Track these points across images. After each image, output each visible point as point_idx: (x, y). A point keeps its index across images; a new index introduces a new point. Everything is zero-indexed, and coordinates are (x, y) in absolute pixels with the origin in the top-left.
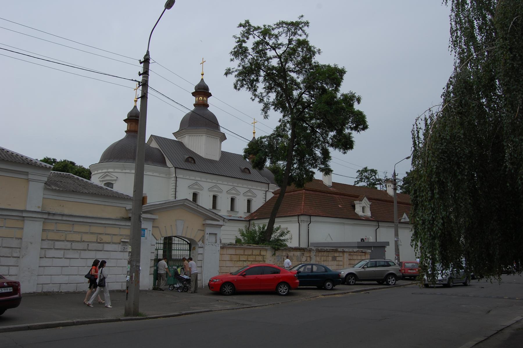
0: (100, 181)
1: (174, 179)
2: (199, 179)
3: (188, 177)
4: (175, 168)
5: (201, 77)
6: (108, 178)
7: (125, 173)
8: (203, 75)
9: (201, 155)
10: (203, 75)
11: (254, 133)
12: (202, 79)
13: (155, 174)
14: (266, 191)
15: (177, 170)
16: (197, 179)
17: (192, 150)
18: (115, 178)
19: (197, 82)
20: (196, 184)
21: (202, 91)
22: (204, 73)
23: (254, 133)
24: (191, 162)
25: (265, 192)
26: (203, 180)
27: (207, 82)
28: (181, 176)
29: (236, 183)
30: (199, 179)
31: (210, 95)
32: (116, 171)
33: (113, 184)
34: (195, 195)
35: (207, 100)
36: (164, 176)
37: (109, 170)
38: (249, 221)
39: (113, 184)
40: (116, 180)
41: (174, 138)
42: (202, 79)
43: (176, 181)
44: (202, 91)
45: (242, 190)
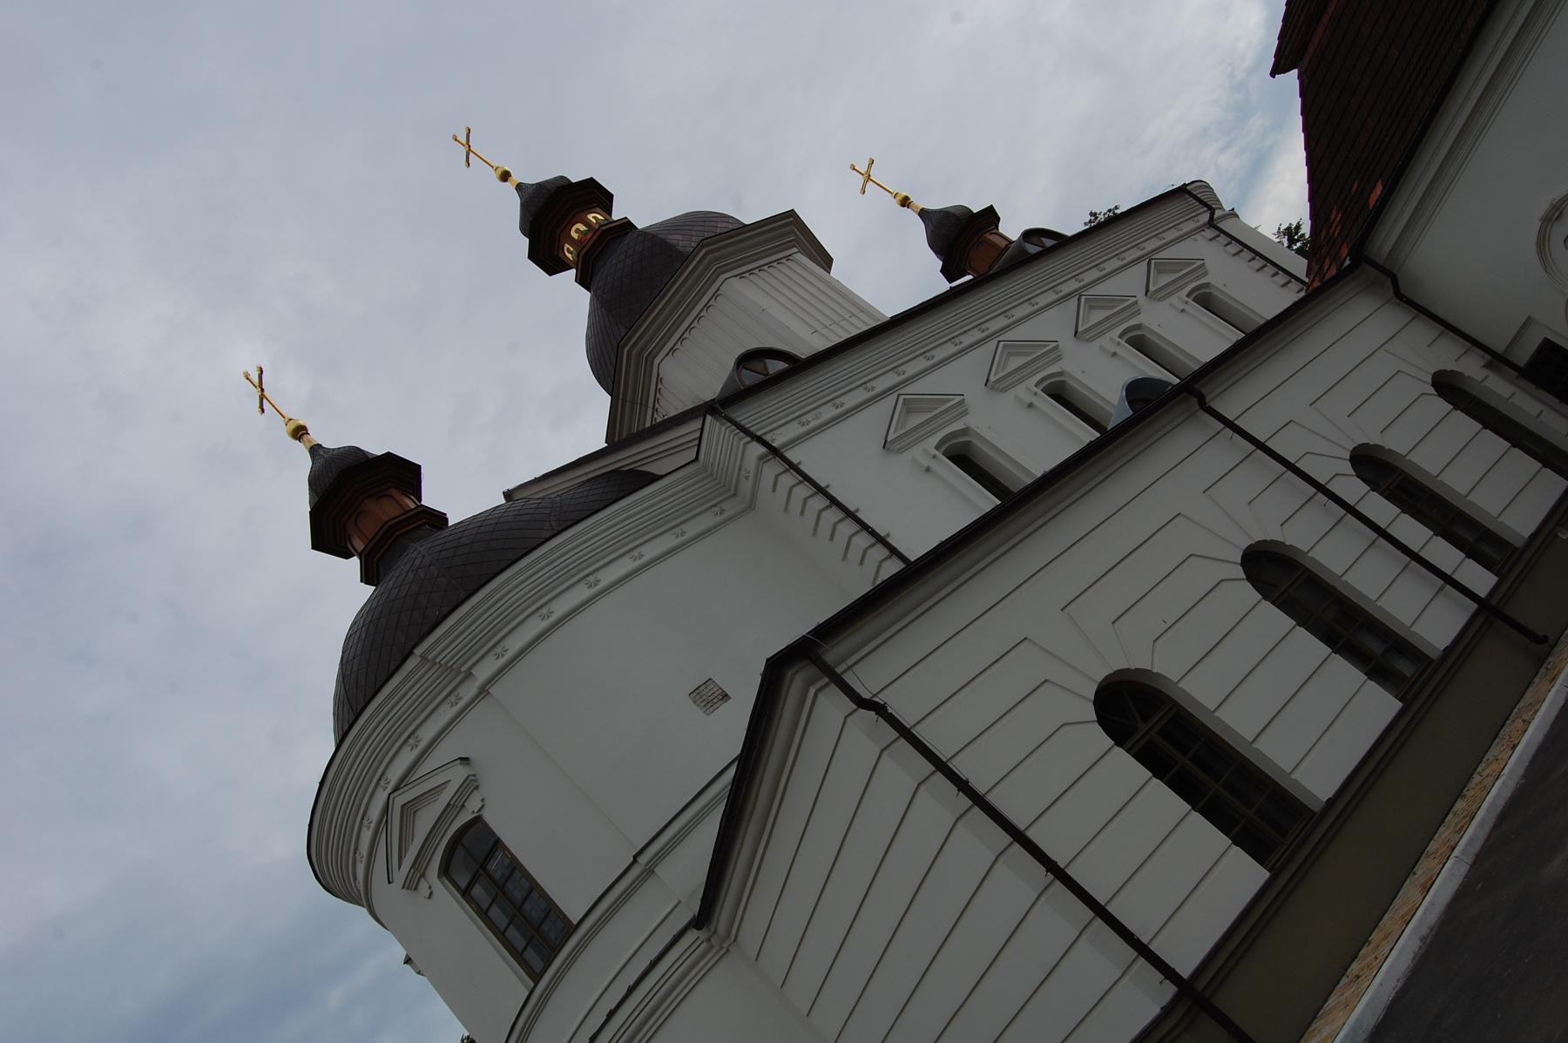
0: (411, 885)
1: (773, 468)
3: (829, 412)
5: (509, 187)
6: (425, 820)
7: (484, 691)
8: (505, 176)
11: (905, 202)
12: (519, 187)
13: (650, 551)
14: (1211, 224)
18: (458, 774)
21: (562, 219)
23: (905, 202)
25: (1210, 233)
26: (912, 369)
28: (794, 430)
31: (594, 194)
32: (427, 734)
33: (478, 820)
34: (964, 457)
36: (708, 520)
37: (394, 775)
38: (1360, 257)
39: (478, 820)
40: (470, 785)
42: (519, 187)
43: (794, 467)
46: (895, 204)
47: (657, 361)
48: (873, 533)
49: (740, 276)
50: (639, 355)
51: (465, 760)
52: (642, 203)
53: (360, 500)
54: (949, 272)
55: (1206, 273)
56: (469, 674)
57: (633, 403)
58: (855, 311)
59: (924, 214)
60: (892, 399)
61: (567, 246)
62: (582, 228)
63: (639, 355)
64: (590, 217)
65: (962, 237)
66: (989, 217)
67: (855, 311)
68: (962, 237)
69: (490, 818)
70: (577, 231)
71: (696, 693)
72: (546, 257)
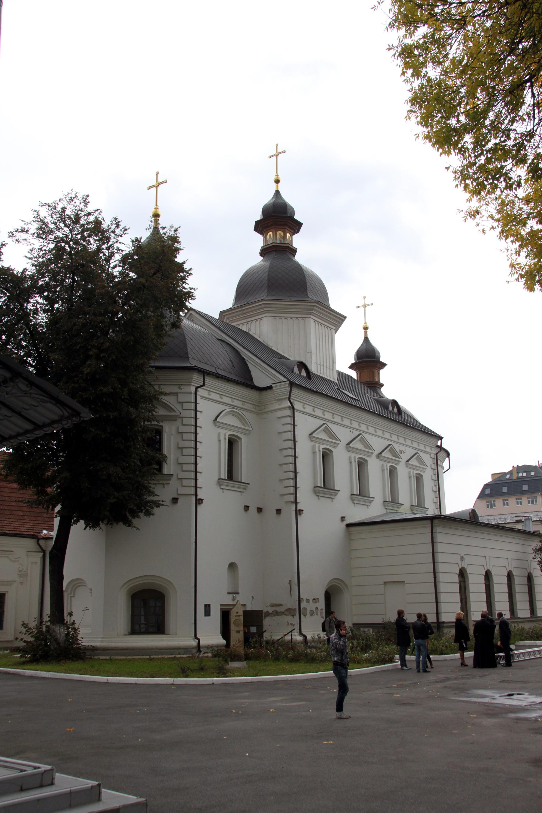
4: (292, 384)
8: (277, 181)
10: (277, 181)
11: (366, 328)
12: (277, 192)
15: (295, 391)
19: (267, 198)
21: (278, 219)
22: (281, 178)
23: (366, 328)
27: (288, 198)
35: (291, 241)
42: (277, 192)
44: (278, 219)
46: (362, 325)
49: (315, 321)
52: (308, 251)
54: (352, 367)
55: (424, 472)
58: (331, 368)
59: (366, 339)
61: (271, 233)
64: (288, 235)
65: (368, 360)
66: (383, 365)
67: (331, 368)
68: (368, 360)
72: (261, 227)
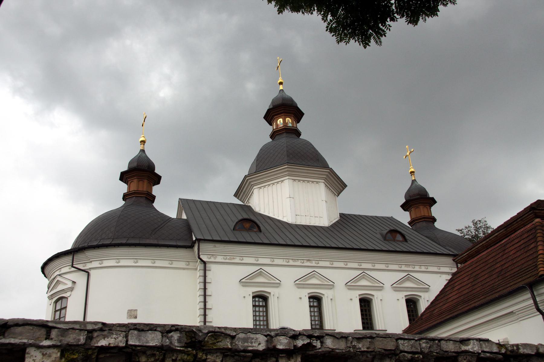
1: (200, 266)
2: (267, 261)
3: (237, 260)
9: (285, 220)
16: (262, 261)
17: (271, 215)
18: (70, 285)
20: (260, 273)
24: (248, 229)
28: (219, 259)
29: (367, 261)
30: (267, 261)
39: (67, 298)
40: (71, 289)
41: (237, 202)
45: (388, 278)
47: (255, 187)
48: (205, 305)
50: (250, 182)
51: (74, 282)
53: (141, 175)
56: (91, 262)
57: (244, 193)
60: (258, 268)
62: (282, 122)
63: (250, 182)
69: (69, 298)
70: (288, 120)
71: (130, 311)
